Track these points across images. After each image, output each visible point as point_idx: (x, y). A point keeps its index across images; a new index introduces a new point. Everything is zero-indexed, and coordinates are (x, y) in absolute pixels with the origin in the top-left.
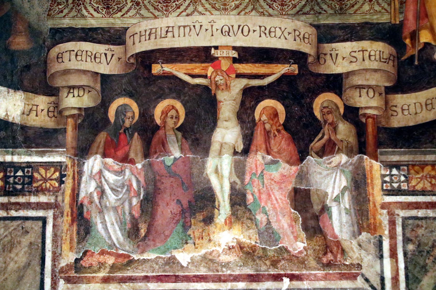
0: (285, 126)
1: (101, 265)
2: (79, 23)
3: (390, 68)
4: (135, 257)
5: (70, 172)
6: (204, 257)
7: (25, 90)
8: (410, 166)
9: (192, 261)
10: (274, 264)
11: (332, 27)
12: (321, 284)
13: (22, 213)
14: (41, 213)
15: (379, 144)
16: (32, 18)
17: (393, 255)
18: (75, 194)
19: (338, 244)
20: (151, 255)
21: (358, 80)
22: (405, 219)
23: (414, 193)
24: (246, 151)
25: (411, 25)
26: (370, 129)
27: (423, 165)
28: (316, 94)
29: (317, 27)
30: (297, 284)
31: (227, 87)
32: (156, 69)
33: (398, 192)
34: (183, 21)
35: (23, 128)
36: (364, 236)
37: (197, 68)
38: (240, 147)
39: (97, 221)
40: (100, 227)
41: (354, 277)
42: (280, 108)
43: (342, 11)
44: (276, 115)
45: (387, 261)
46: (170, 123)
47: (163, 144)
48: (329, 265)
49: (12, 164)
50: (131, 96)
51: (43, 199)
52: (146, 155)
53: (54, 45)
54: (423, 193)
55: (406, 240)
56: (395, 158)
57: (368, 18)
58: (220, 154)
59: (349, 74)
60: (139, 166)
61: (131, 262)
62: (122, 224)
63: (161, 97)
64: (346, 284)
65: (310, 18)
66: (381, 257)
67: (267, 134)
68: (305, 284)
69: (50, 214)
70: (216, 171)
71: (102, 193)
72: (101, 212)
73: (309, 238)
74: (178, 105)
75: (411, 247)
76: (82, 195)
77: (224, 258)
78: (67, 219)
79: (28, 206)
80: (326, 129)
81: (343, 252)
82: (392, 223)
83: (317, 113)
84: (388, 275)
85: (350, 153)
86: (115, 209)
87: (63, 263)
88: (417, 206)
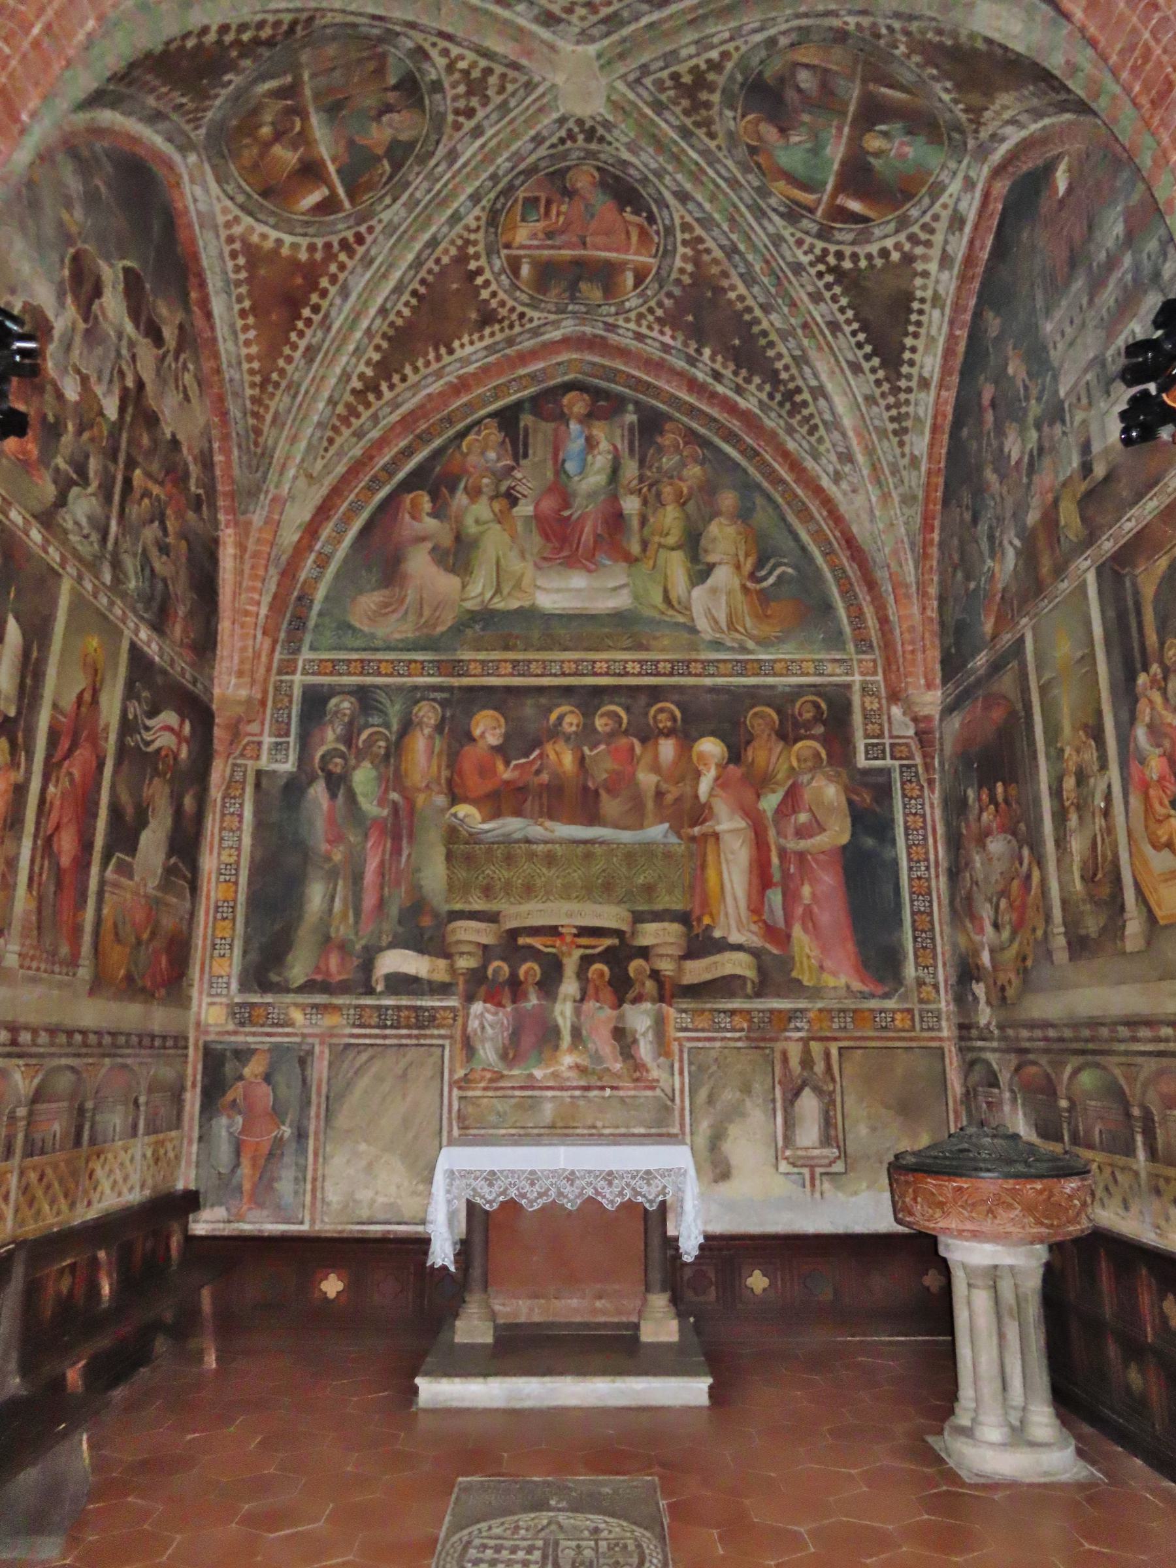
0: (610, 983)
1: (482, 1078)
2: (467, 907)
3: (683, 942)
4: (505, 1072)
5: (460, 1013)
6: (553, 1073)
7: (430, 954)
8: (694, 1011)
9: (545, 1076)
10: (600, 1079)
11: (642, 912)
12: (632, 1093)
13: (428, 1042)
14: (440, 1042)
15: (673, 996)
16: (435, 903)
17: (681, 1073)
18: (465, 1026)
19: (644, 1065)
20: (515, 1072)
21: (662, 951)
22: (690, 1049)
23: (696, 1030)
24: (582, 1000)
25: (697, 912)
26: (667, 986)
27: (703, 1011)
28: (631, 958)
29: (633, 912)
30: (615, 1093)
31: (570, 955)
32: (522, 941)
33: (686, 1030)
34: (540, 906)
35: (430, 982)
36: (662, 1059)
37: (549, 940)
38: (578, 997)
39: (479, 1047)
40: (481, 1052)
41: (653, 1088)
42: (605, 969)
43: (650, 901)
44: (602, 974)
45: (677, 1077)
46: (530, 980)
47: (525, 996)
48: (637, 1080)
49: (421, 1008)
50: (503, 959)
51: (442, 1032)
52: (514, 1002)
53: (450, 921)
54: (703, 1030)
55: (690, 1063)
56: (684, 1006)
57: (667, 906)
58: (565, 1000)
59: (653, 946)
60: (509, 1009)
61: (502, 1077)
62: (496, 1050)
63: (525, 961)
64: (649, 1093)
65: (627, 906)
66: (673, 1074)
67: (597, 989)
68: (621, 1093)
69: (447, 1043)
70: (562, 1014)
71: (483, 1028)
72: (483, 1041)
73: (624, 1061)
74: (536, 967)
75: (693, 1068)
76: (469, 1029)
77: (567, 1074)
78: (459, 1046)
79: (432, 1036)
80: (637, 985)
81: (648, 1071)
82: (681, 1051)
83: (632, 974)
84: (677, 1086)
85: (654, 1001)
86: (492, 1039)
87: (456, 1077)
88: (698, 1039)
